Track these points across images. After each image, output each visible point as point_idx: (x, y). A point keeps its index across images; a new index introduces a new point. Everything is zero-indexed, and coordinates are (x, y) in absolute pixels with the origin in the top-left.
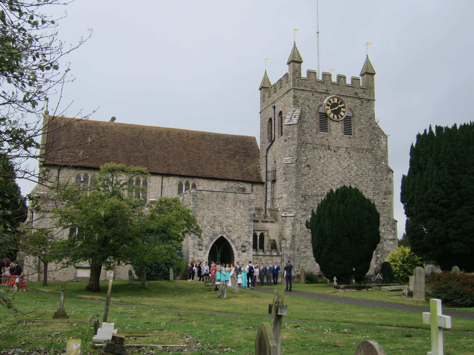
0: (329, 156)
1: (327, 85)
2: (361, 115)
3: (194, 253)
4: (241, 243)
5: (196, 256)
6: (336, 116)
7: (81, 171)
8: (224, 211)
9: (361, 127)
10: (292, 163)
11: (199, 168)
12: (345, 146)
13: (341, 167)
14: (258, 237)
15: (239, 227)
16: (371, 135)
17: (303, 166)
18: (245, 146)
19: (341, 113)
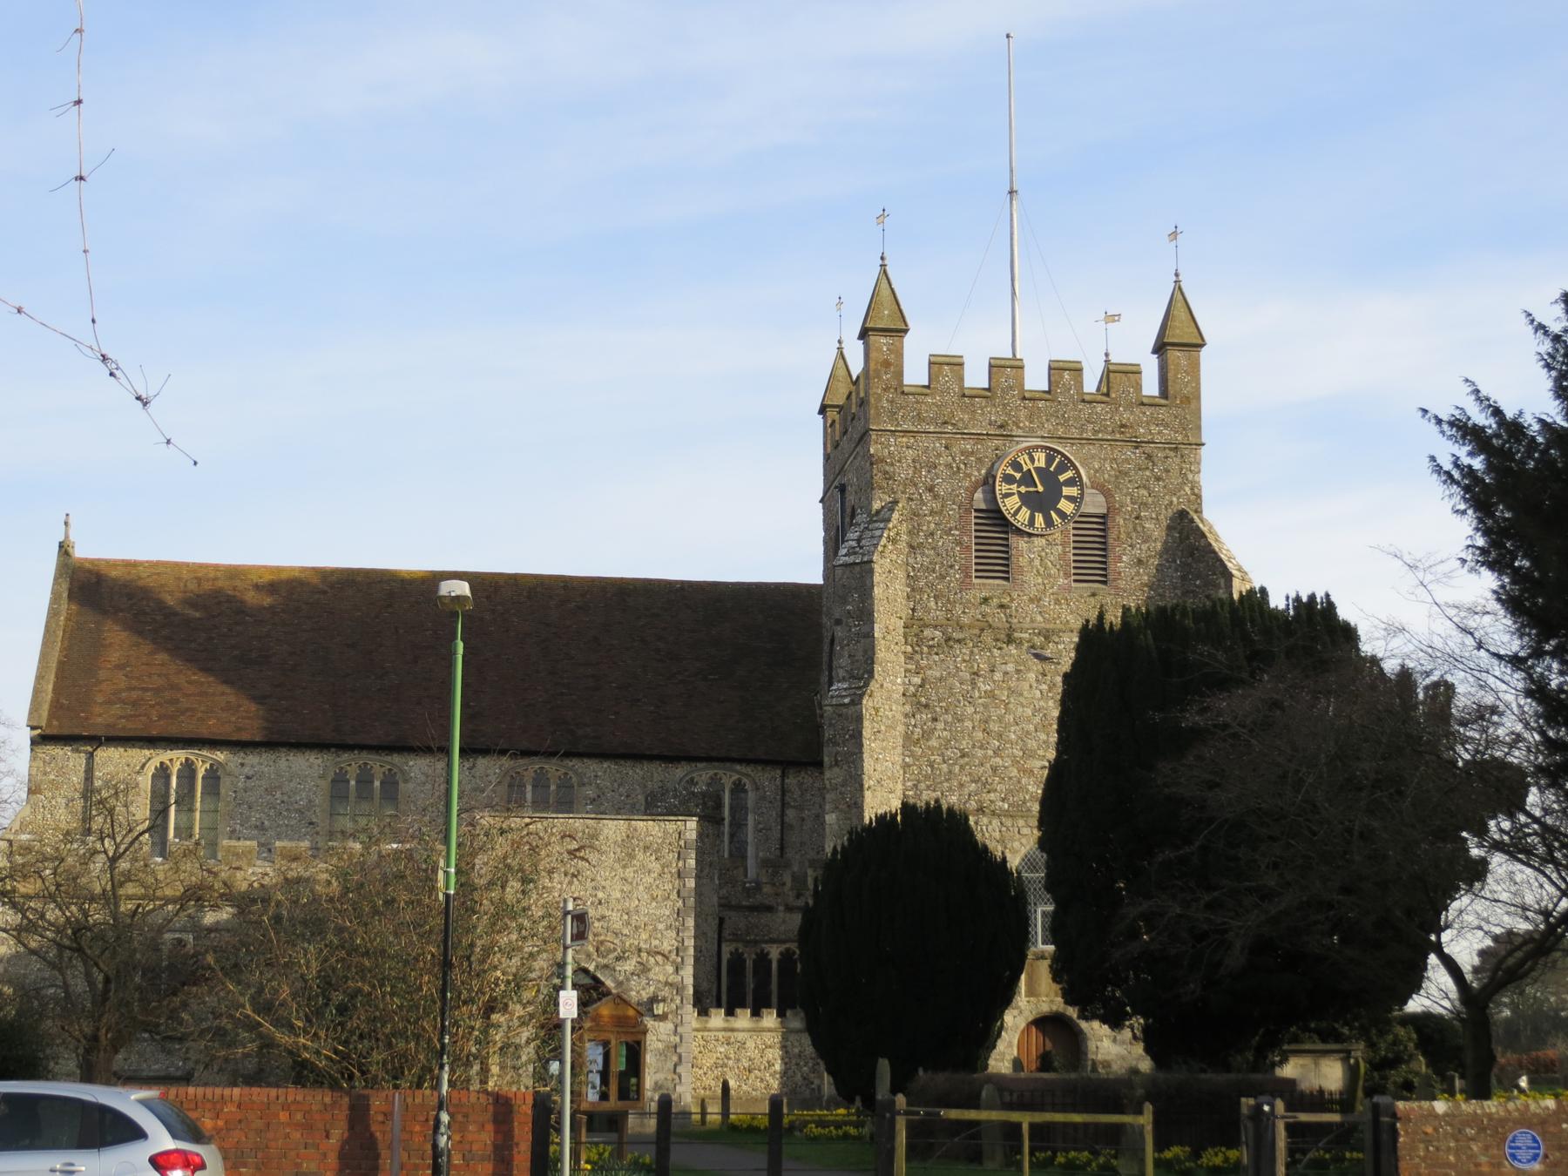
0: (1010, 667)
6: (1039, 518)
14: (774, 965)
16: (1183, 578)
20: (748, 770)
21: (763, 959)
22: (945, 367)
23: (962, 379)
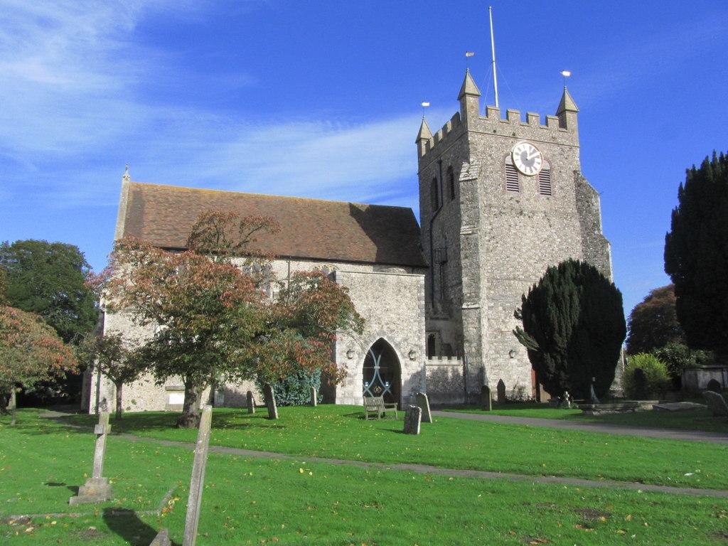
0: (521, 224)
9: (562, 184)
13: (539, 239)
17: (487, 238)
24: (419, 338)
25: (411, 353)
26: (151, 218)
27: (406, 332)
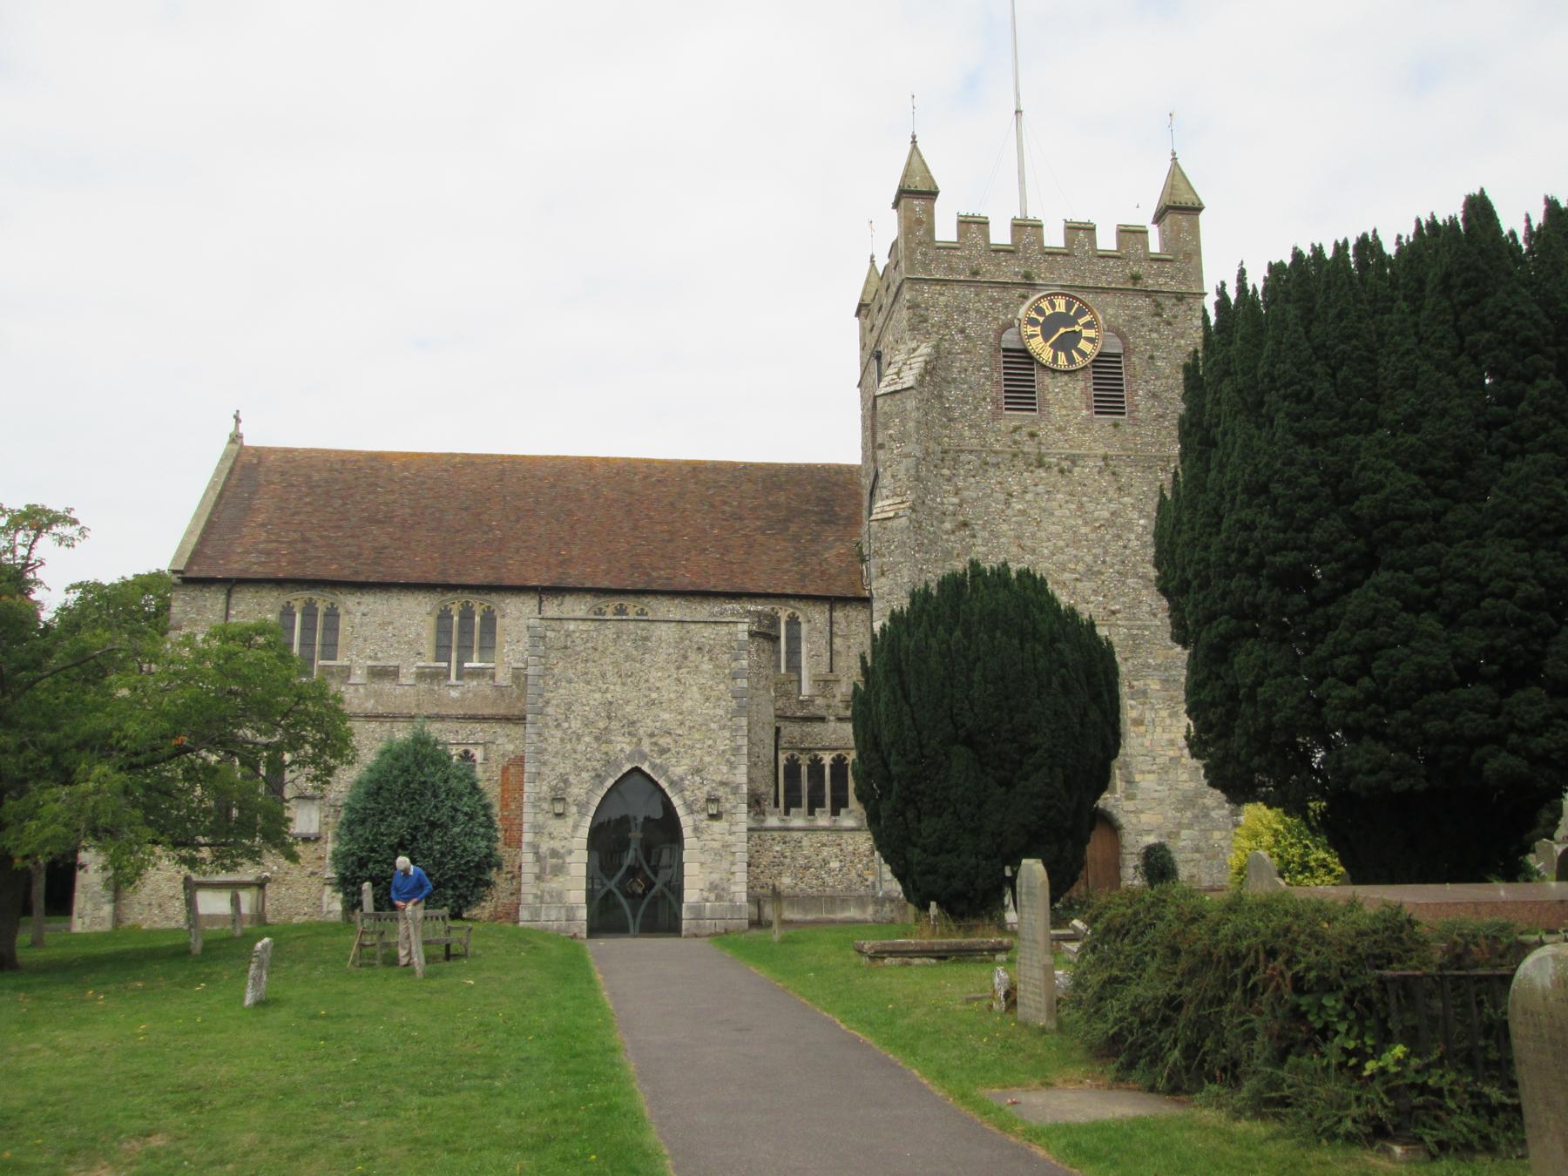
1: (1027, 259)
2: (1157, 347)
3: (538, 830)
4: (706, 788)
5: (546, 838)
6: (1062, 357)
7: (296, 595)
8: (643, 685)
9: (1157, 385)
10: (896, 516)
11: (662, 565)
12: (1101, 452)
14: (827, 771)
15: (697, 736)
17: (948, 526)
18: (825, 494)
19: (1083, 345)
20: (801, 605)
21: (816, 766)
22: (972, 225)
23: (987, 236)
24: (732, 766)
25: (712, 800)
26: (260, 519)
27: (698, 752)
